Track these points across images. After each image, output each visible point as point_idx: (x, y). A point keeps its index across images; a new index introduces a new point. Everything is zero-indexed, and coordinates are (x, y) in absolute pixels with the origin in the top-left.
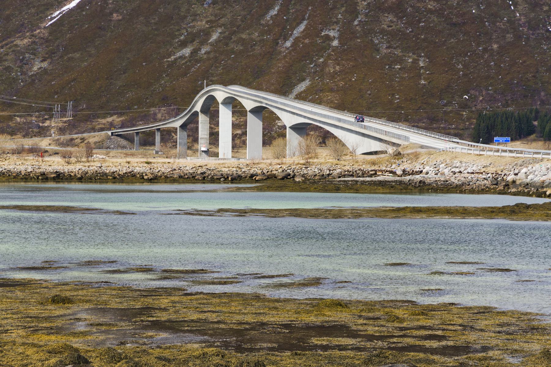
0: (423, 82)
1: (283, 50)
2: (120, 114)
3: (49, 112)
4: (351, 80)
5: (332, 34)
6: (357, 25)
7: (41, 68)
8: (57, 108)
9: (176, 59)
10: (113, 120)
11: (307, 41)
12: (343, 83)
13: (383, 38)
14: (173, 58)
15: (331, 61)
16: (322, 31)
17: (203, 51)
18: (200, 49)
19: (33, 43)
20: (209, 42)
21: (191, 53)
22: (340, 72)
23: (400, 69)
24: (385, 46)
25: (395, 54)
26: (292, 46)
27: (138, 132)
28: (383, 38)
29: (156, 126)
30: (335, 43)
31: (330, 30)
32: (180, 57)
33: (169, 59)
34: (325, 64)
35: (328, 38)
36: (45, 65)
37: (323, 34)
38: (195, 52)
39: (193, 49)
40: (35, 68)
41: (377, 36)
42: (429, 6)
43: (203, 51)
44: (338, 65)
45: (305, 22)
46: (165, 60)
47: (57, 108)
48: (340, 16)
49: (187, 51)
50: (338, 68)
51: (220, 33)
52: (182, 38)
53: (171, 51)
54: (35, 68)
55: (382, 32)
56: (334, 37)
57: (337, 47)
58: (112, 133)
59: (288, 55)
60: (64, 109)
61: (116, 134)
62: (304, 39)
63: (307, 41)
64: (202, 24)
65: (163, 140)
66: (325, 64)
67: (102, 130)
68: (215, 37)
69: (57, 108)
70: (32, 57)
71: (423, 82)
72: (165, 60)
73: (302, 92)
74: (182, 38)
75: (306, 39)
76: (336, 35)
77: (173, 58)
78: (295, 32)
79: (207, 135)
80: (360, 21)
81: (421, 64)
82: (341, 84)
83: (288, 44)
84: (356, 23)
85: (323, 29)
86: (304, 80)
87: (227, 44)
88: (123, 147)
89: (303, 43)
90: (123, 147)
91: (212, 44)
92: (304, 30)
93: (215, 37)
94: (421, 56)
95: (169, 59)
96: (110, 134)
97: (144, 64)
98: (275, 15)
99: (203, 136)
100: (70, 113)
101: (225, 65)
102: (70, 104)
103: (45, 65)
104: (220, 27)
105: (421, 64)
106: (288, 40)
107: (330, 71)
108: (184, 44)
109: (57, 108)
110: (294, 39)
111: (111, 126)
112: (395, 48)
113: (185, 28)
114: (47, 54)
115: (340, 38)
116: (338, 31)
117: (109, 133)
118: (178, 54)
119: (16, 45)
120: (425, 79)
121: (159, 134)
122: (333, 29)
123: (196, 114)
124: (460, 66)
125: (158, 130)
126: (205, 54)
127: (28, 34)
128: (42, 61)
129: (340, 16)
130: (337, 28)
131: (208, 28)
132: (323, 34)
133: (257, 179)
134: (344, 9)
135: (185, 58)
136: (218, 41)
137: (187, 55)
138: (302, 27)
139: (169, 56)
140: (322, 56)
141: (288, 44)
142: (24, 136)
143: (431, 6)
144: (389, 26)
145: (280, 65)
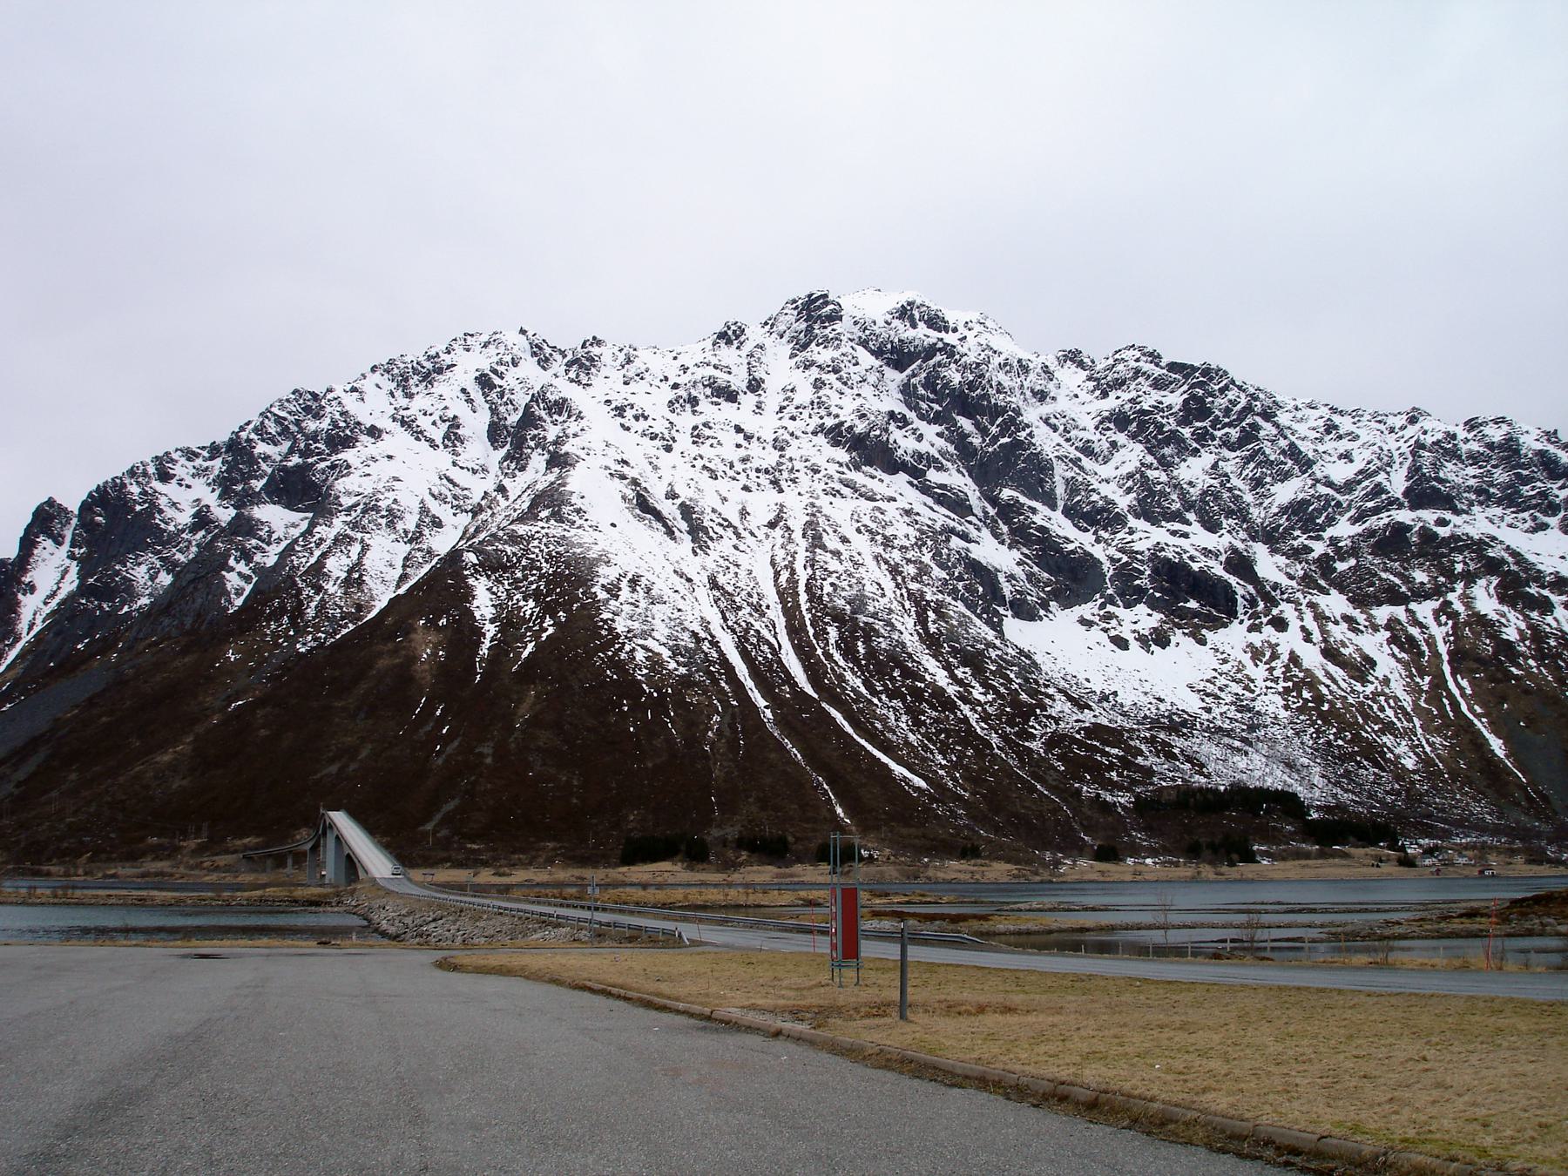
0: (575, 801)
2: (258, 836)
3: (185, 835)
9: (322, 778)
11: (460, 758)
14: (319, 775)
19: (175, 759)
24: (539, 764)
30: (489, 760)
32: (326, 775)
35: (481, 755)
36: (184, 783)
37: (477, 751)
38: (341, 769)
40: (174, 786)
45: (459, 739)
48: (495, 733)
49: (333, 769)
50: (489, 786)
52: (331, 754)
60: (199, 829)
65: (294, 863)
67: (235, 852)
68: (364, 754)
71: (575, 801)
73: (449, 812)
77: (319, 775)
80: (516, 738)
82: (491, 802)
84: (512, 739)
86: (453, 798)
92: (458, 746)
93: (364, 754)
94: (575, 774)
100: (205, 833)
102: (205, 825)
103: (184, 783)
105: (575, 783)
108: (332, 761)
111: (246, 848)
118: (324, 772)
119: (156, 762)
120: (577, 798)
124: (614, 785)
125: (290, 852)
128: (183, 778)
129: (495, 733)
134: (500, 725)
138: (456, 743)
142: (153, 860)
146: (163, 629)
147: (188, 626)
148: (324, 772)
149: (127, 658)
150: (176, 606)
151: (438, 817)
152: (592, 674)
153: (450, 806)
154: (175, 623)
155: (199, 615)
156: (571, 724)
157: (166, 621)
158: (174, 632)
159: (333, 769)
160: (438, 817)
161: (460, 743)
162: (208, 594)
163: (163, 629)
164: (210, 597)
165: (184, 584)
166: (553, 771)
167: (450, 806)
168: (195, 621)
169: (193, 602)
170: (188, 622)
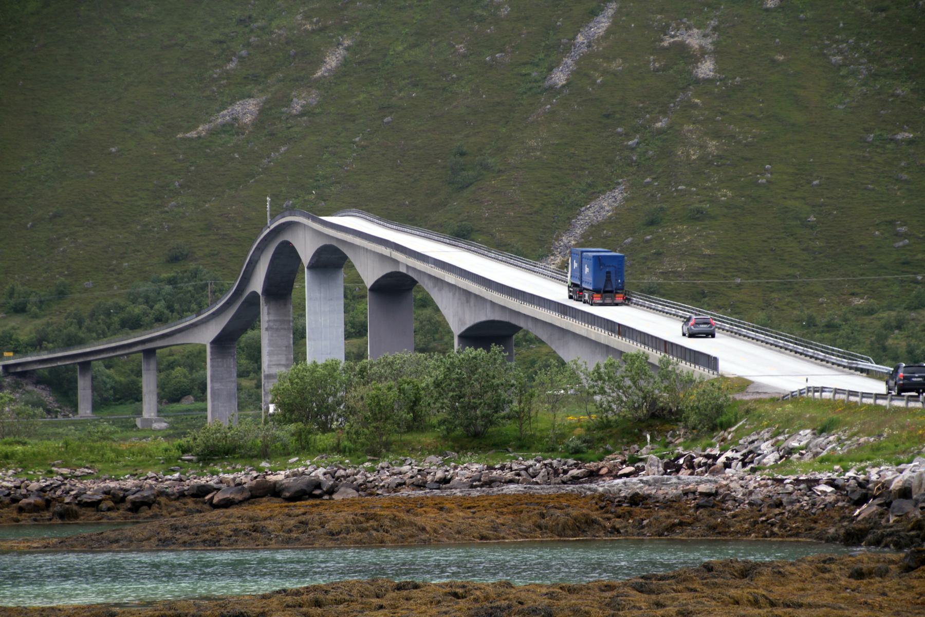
5: (694, 40)
9: (213, 133)
11: (616, 65)
12: (729, 193)
13: (855, 48)
15: (691, 127)
16: (664, 30)
17: (297, 106)
20: (319, 74)
21: (261, 111)
23: (911, 142)
27: (89, 363)
28: (855, 48)
30: (706, 69)
33: (193, 134)
39: (265, 103)
41: (837, 42)
44: (717, 135)
46: (180, 135)
51: (347, 49)
56: (703, 52)
61: (19, 369)
63: (616, 65)
72: (180, 135)
75: (614, 58)
76: (708, 43)
78: (580, 39)
79: (287, 366)
83: (559, 77)
85: (668, 26)
86: (610, 185)
89: (605, 72)
92: (608, 32)
95: (193, 134)
99: (276, 370)
101: (364, 147)
107: (688, 156)
115: (718, 53)
118: (223, 117)
131: (313, 31)
133: (215, 500)
135: (240, 131)
136: (343, 72)
137: (248, 119)
138: (602, 25)
140: (664, 112)
141: (559, 77)
145: (533, 143)
148: (223, 117)
161: (615, 23)
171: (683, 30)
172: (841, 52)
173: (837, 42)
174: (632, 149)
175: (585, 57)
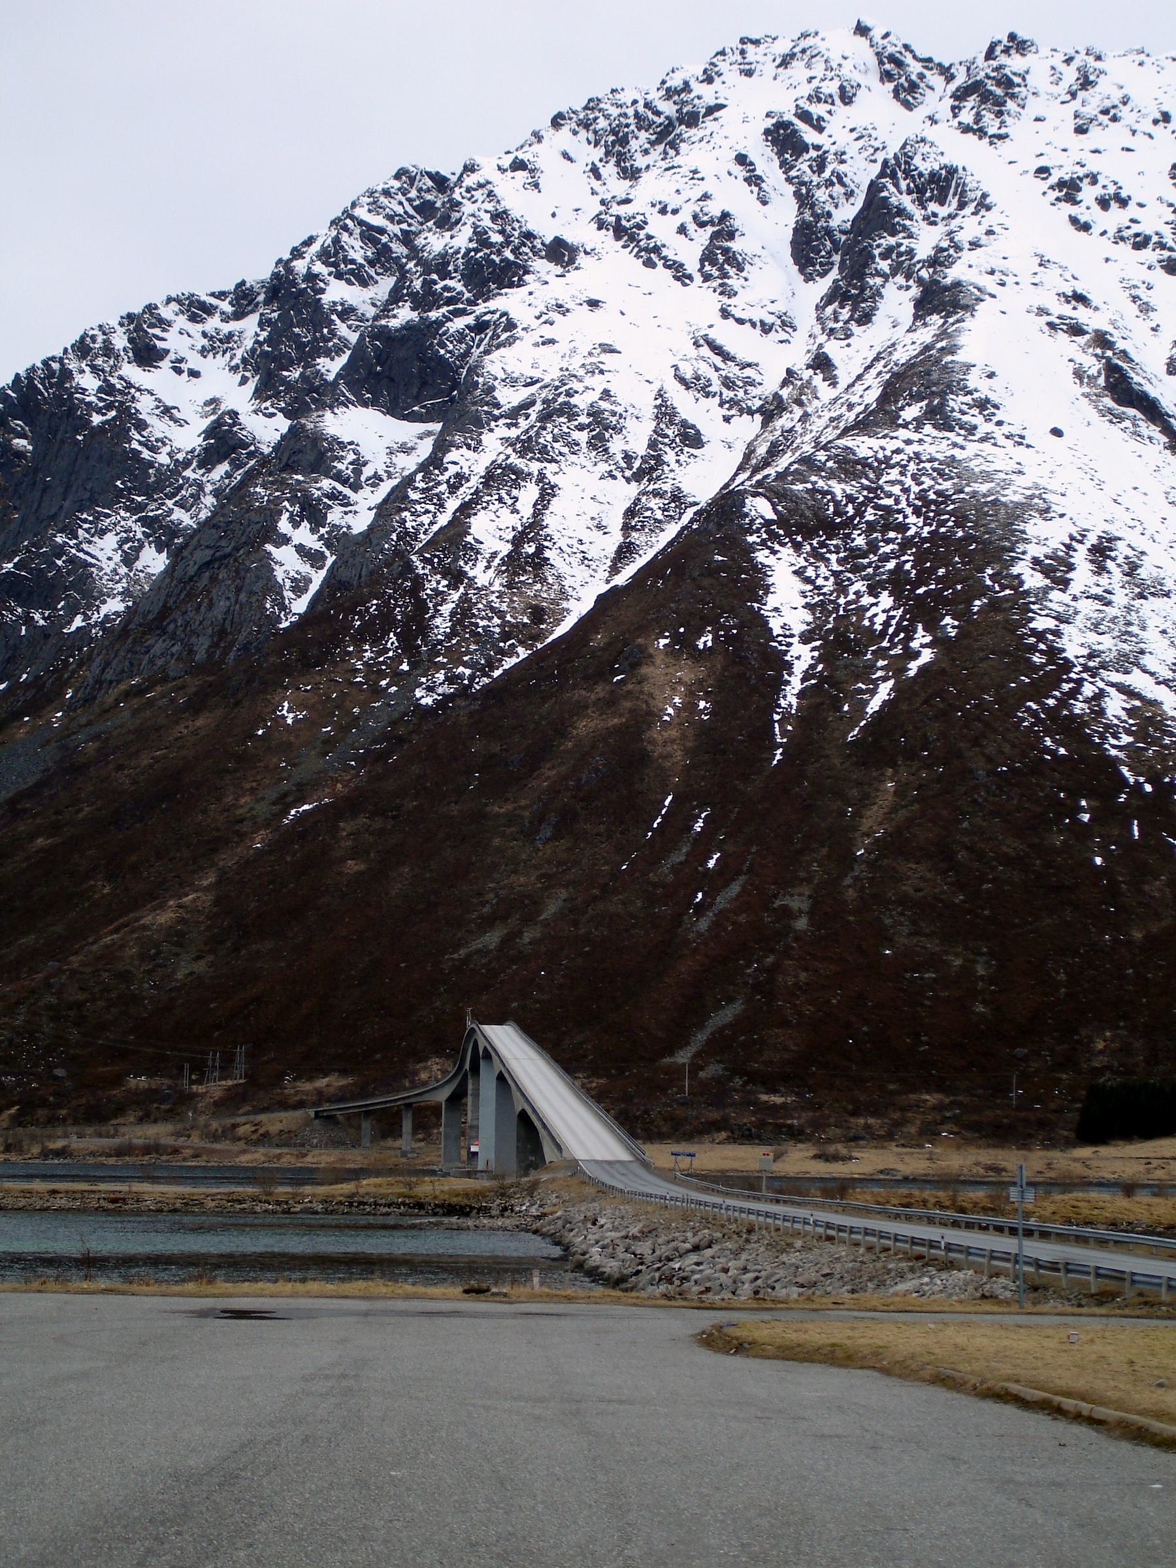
0: (980, 1009)
1: (691, 936)
2: (344, 1073)
3: (201, 1071)
4: (828, 1002)
6: (849, 886)
7: (191, 974)
8: (214, 1060)
9: (469, 956)
10: (327, 1086)
12: (812, 1009)
14: (463, 952)
16: (775, 896)
17: (527, 937)
18: (520, 933)
19: (182, 921)
22: (807, 984)
25: (926, 948)
26: (710, 929)
28: (902, 914)
29: (403, 1098)
30: (802, 924)
31: (792, 895)
32: (478, 951)
33: (455, 956)
34: (775, 968)
35: (786, 912)
37: (777, 903)
39: (507, 934)
40: (179, 975)
42: (1004, 849)
43: (527, 937)
44: (806, 969)
45: (743, 878)
47: (214, 1060)
48: (815, 867)
49: (492, 939)
50: (803, 976)
52: (486, 910)
53: (460, 939)
54: (179, 975)
55: (903, 901)
56: (800, 911)
57: (805, 932)
58: (316, 1112)
59: (702, 947)
60: (227, 1063)
62: (737, 915)
63: (742, 918)
64: (524, 881)
65: (416, 1128)
66: (775, 968)
67: (300, 1105)
68: (552, 908)
69: (214, 1058)
70: (175, 949)
71: (980, 1009)
73: (724, 1027)
74: (486, 910)
76: (805, 906)
77: (463, 952)
78: (718, 898)
80: (856, 879)
81: (981, 971)
82: (808, 1010)
84: (848, 881)
86: (731, 1000)
87: (575, 924)
88: (338, 1142)
89: (733, 923)
90: (338, 1142)
91: (546, 924)
92: (739, 896)
93: (552, 908)
95: (455, 956)
96: (312, 1115)
97: (403, 965)
98: (681, 863)
102: (241, 1051)
103: (200, 967)
104: (566, 886)
106: (704, 915)
108: (487, 923)
109: (214, 1058)
110: (715, 915)
111: (321, 1097)
112: (926, 935)
113: (493, 889)
114: (206, 944)
115: (811, 913)
116: (810, 897)
117: (311, 1113)
118: (477, 945)
119: (144, 928)
121: (410, 1115)
122: (800, 895)
123: (465, 1075)
124: (1062, 976)
125: (409, 1106)
126: (530, 943)
127: (171, 903)
128: (198, 958)
130: (807, 893)
132: (777, 903)
134: (824, 851)
138: (735, 888)
139: (457, 947)
140: (772, 951)
142: (141, 1120)
143: (1009, 847)
144: (918, 890)
146: (151, 662)
147: (200, 656)
149: (83, 721)
150: (177, 615)
151: (701, 1037)
152: (1014, 746)
153: (727, 1015)
154: (174, 649)
155: (222, 633)
156: (970, 849)
157: (159, 647)
158: (174, 668)
159: (492, 939)
160: (701, 1037)
161: (744, 889)
162: (239, 590)
163: (151, 662)
164: (243, 597)
165: (192, 571)
166: (933, 946)
167: (727, 1015)
168: (215, 645)
169: (211, 605)
170: (202, 646)
171: (788, 897)
172: (891, 916)
173: (889, 910)
174: (749, 975)
175: (721, 912)
